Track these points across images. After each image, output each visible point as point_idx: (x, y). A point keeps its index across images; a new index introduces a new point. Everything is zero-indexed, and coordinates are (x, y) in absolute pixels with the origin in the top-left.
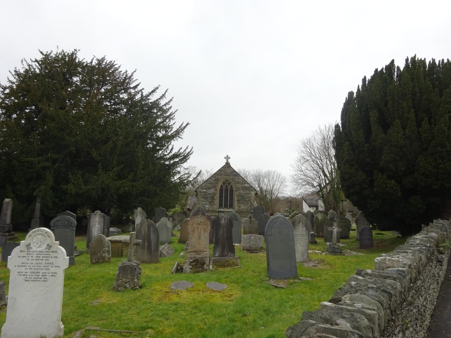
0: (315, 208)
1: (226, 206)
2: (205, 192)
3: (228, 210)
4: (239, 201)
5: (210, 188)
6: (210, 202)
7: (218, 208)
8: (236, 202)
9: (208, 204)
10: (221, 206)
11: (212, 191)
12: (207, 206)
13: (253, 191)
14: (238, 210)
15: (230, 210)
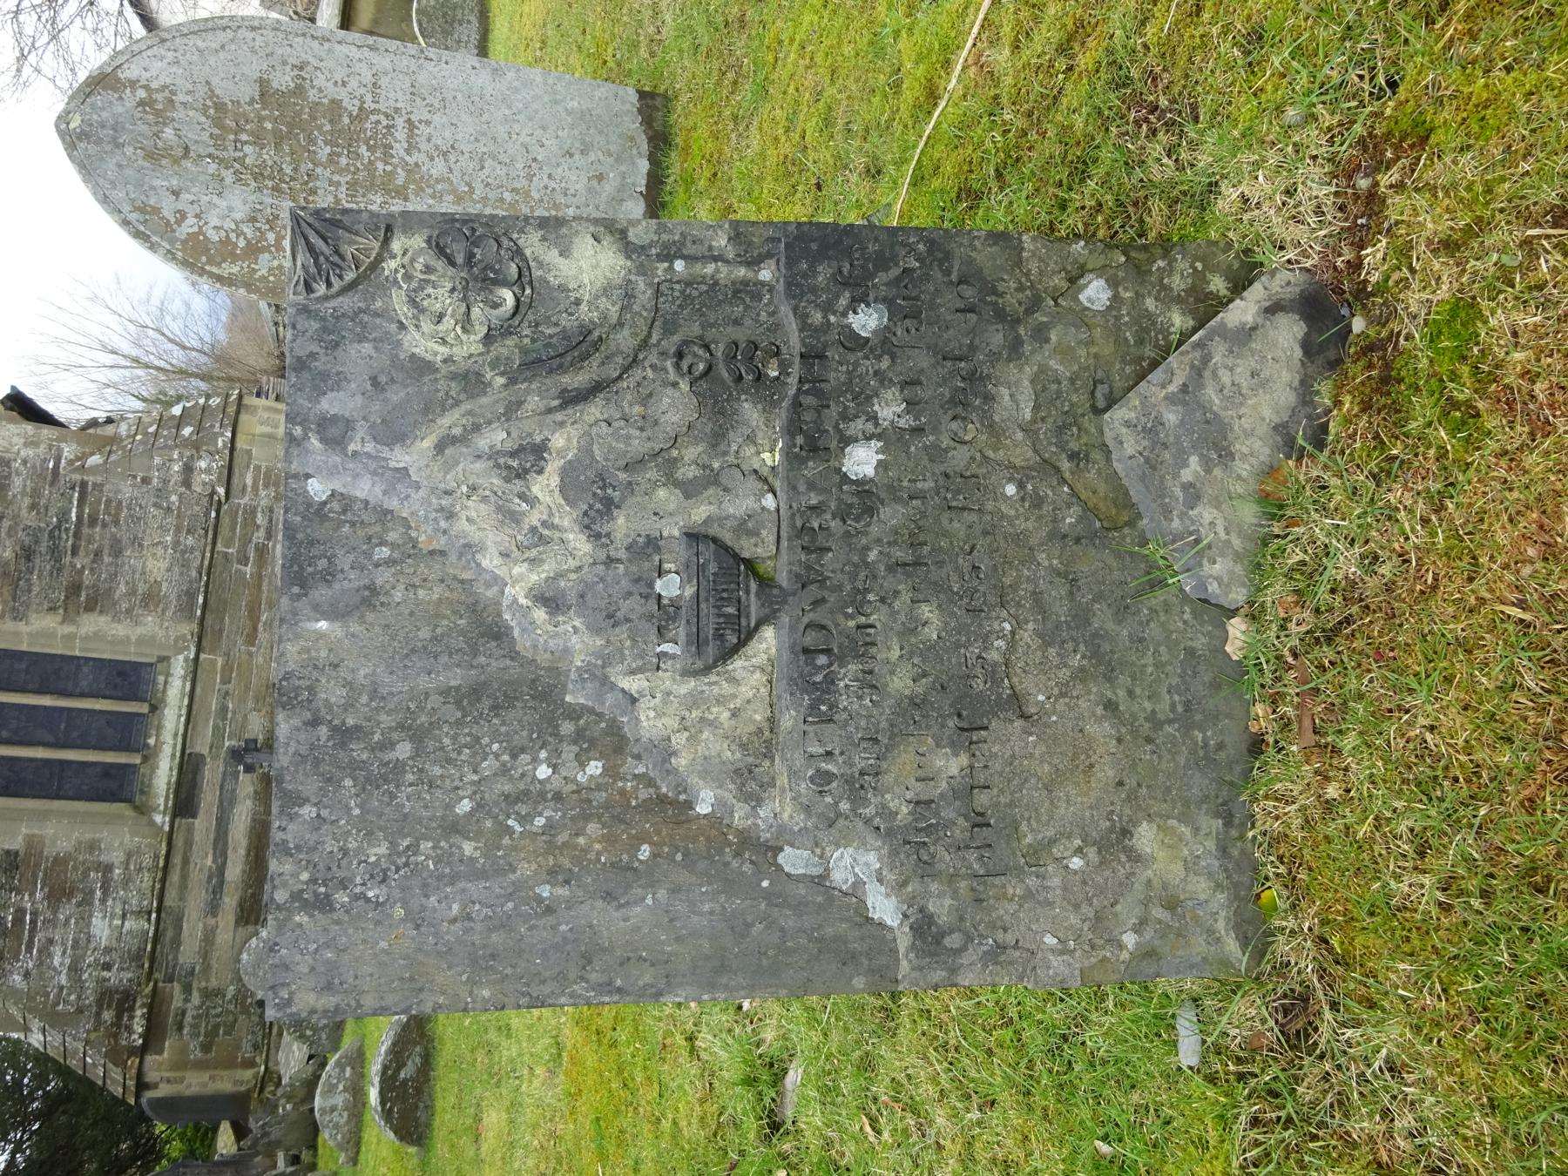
1: (130, 734)
3: (172, 718)
4: (79, 598)
6: (58, 894)
7: (143, 810)
8: (91, 624)
9: (84, 920)
10: (117, 787)
12: (101, 929)
15: (175, 689)
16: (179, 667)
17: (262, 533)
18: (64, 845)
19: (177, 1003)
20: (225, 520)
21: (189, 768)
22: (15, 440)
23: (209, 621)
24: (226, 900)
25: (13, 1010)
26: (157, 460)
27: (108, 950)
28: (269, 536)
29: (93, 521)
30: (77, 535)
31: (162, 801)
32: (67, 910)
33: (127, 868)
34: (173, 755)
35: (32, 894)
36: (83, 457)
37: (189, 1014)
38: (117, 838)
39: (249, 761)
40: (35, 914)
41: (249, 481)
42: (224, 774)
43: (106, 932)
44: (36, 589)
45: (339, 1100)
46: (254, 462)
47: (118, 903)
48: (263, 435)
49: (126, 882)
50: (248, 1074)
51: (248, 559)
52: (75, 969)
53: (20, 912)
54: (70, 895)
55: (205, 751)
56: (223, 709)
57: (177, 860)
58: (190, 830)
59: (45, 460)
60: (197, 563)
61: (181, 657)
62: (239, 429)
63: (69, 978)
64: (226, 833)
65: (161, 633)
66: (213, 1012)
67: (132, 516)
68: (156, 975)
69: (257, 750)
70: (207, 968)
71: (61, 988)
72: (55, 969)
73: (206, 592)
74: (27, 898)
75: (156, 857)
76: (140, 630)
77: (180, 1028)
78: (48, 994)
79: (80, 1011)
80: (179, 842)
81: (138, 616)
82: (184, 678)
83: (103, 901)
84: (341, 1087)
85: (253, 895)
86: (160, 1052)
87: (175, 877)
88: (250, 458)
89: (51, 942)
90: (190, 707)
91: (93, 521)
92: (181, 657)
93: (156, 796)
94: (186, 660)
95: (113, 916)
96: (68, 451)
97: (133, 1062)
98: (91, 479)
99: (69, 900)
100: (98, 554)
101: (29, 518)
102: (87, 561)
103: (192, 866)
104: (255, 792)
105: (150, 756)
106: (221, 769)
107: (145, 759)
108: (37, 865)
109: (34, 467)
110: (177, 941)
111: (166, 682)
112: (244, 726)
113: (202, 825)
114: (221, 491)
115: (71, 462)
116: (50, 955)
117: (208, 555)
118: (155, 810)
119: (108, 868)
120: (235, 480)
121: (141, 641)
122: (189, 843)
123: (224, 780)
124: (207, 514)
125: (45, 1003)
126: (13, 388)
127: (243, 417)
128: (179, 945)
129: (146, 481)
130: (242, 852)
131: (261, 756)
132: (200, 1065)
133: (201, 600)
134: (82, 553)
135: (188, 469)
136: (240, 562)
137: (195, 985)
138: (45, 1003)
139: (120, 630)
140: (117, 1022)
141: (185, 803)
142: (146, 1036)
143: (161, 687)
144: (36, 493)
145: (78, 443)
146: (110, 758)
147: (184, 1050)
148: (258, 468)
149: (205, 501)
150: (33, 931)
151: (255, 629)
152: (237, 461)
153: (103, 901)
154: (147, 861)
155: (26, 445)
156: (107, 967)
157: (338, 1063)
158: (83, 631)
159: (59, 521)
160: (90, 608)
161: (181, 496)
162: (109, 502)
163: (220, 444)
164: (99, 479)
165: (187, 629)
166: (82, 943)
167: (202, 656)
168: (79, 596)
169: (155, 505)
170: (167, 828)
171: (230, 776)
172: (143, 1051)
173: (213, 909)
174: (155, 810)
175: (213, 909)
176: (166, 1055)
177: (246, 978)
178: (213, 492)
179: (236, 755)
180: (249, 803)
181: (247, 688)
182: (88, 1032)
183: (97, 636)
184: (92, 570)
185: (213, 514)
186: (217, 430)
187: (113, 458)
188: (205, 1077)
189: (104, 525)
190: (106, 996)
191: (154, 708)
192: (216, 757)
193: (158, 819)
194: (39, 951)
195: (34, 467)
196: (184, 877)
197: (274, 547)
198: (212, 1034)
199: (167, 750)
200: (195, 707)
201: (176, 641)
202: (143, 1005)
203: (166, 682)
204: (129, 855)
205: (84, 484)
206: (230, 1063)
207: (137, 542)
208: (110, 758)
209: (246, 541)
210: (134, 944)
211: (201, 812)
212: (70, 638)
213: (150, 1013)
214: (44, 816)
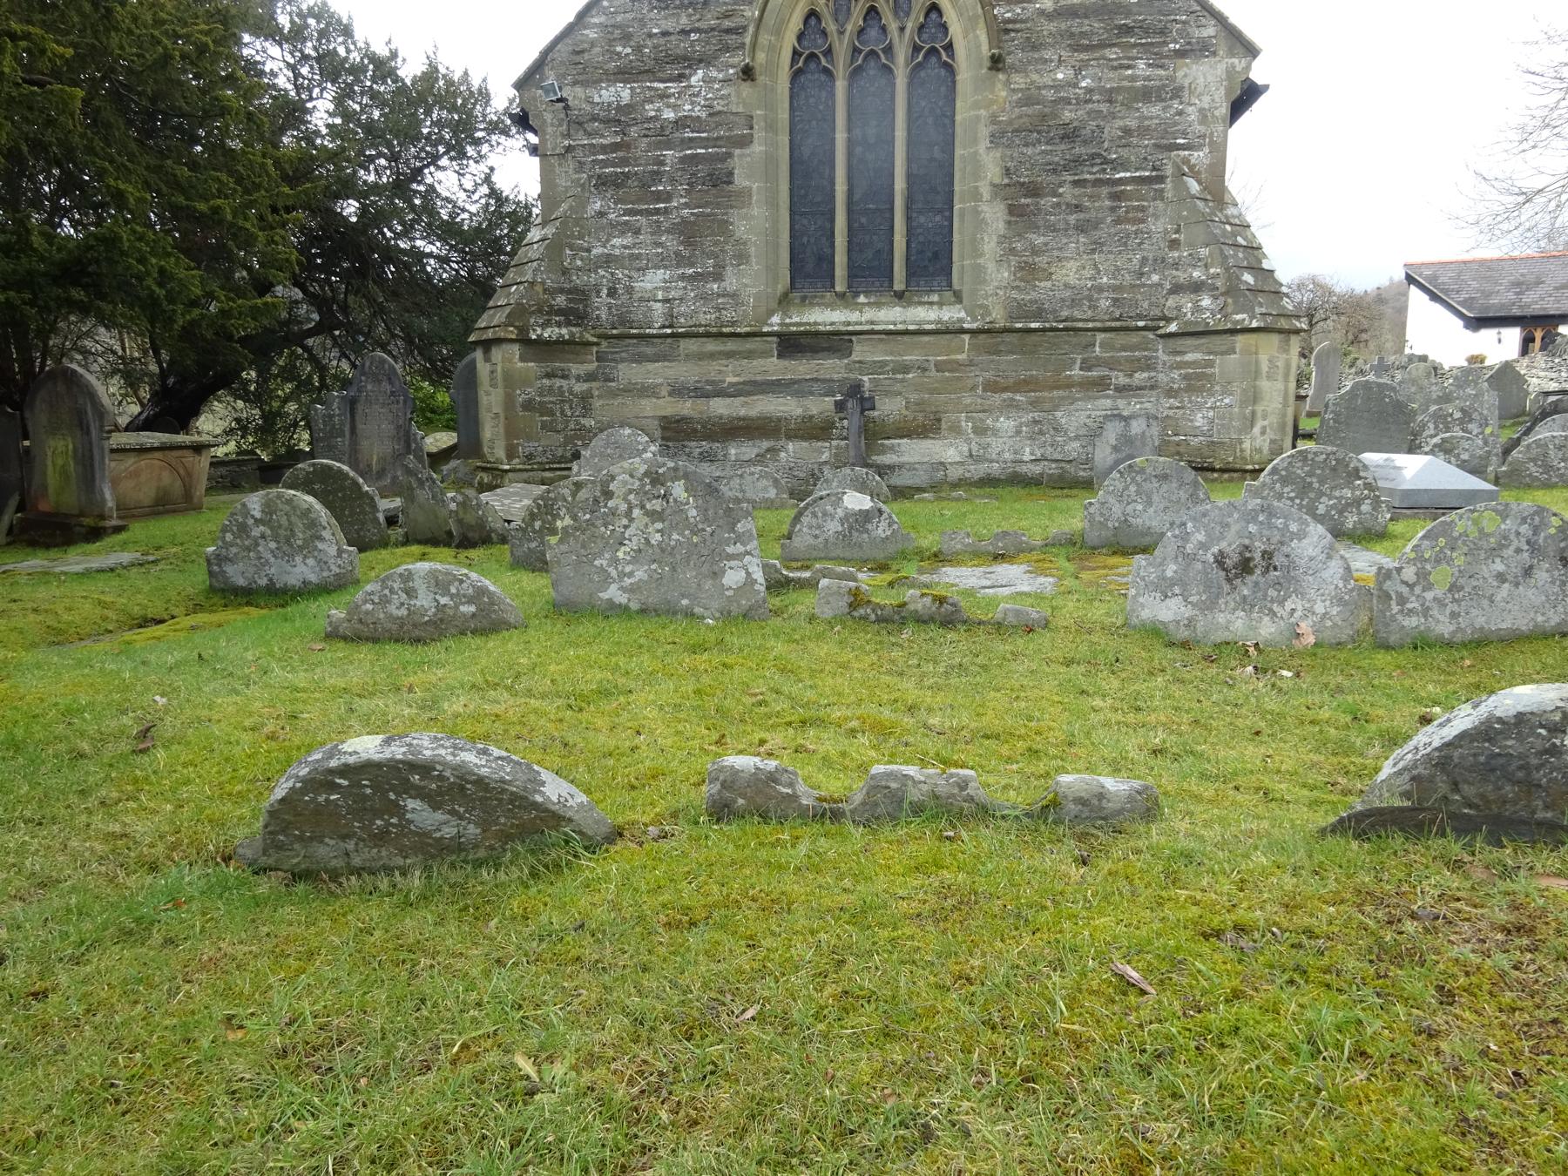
0: (1513, 335)
1: (870, 274)
2: (619, 118)
3: (891, 315)
4: (1023, 199)
5: (674, 63)
6: (688, 232)
7: (784, 302)
8: (995, 215)
10: (808, 270)
11: (701, 91)
12: (653, 281)
13: (1202, 50)
14: (1020, 311)
15: (924, 314)
16: (951, 314)
17: (1122, 380)
18: (741, 228)
19: (576, 369)
20: (1134, 338)
21: (836, 342)
22: (1206, 99)
23: (1008, 338)
24: (689, 404)
25: (564, 206)
26: (1204, 252)
27: (630, 290)
28: (1121, 390)
29: (1116, 197)
30: (1098, 183)
31: (796, 319)
32: (671, 242)
33: (719, 296)
34: (849, 324)
35: (686, 205)
36: (1196, 175)
37: (564, 383)
38: (752, 281)
39: (849, 405)
40: (666, 211)
41: (1189, 357)
42: (833, 380)
43: (649, 286)
44: (1029, 151)
45: (425, 601)
46: (1218, 360)
47: (681, 292)
48: (1257, 363)
49: (704, 297)
50: (500, 453)
51: (1089, 369)
52: (608, 260)
53: (668, 197)
54: (688, 243)
55: (855, 357)
56: (905, 369)
57: (731, 345)
58: (765, 354)
59: (1184, 134)
60: (1077, 314)
61: (963, 314)
62: (1262, 336)
63: (599, 256)
64: (763, 392)
65: (990, 289)
66: (567, 407)
67: (1128, 236)
68: (604, 343)
69: (862, 412)
70: (614, 394)
71: (588, 250)
72: (608, 241)
73: (1044, 330)
74: (683, 201)
75: (733, 324)
76: (991, 266)
77: (548, 376)
78: (581, 237)
79: (565, 272)
80: (750, 345)
81: (1009, 262)
82: (939, 322)
83: (683, 277)
84: (443, 601)
85: (695, 431)
86: (522, 359)
87: (711, 346)
88: (1223, 353)
89: (637, 232)
90: (906, 332)
91: (1116, 197)
92: (963, 314)
93: (800, 314)
94: (961, 320)
95: (666, 289)
96: (1199, 157)
97: (512, 333)
98: (1168, 185)
99: (682, 243)
100: (1078, 208)
101: (1112, 129)
102: (1069, 198)
103: (724, 362)
104: (811, 417)
105: (845, 300)
106: (835, 376)
107: (842, 296)
108: (718, 205)
109: (1176, 124)
110: (640, 359)
111: (931, 303)
112: (887, 393)
113: (773, 366)
114: (1173, 328)
115: (1186, 161)
116: (623, 233)
117: (1090, 325)
118: (785, 314)
119: (718, 277)
120: (1190, 341)
121: (979, 270)
122: (750, 355)
123: (824, 381)
124: (1140, 317)
125: (572, 236)
126: (1266, 87)
127: (1275, 339)
128: (639, 362)
129: (1174, 244)
130: (743, 412)
131: (856, 418)
132: (509, 402)
133: (1033, 325)
134: (1077, 191)
135: (1197, 287)
136: (1084, 361)
137: (594, 384)
138: (572, 236)
139: (990, 246)
140: (554, 311)
141: (792, 344)
142: (540, 342)
143: (926, 299)
144: (1143, 131)
145: (1210, 165)
146: (840, 259)
147: (526, 382)
148: (1210, 364)
149: (1157, 312)
150: (649, 213)
151: (1005, 389)
152: (1217, 339)
153: (683, 277)
154: (728, 315)
155: (1201, 110)
156: (612, 293)
157: (482, 591)
158: (984, 207)
159: (1113, 161)
160: (1012, 210)
161: (1159, 285)
162: (1143, 209)
163: (1238, 317)
164: (1169, 194)
165: (998, 316)
166: (637, 264)
167: (966, 337)
168: (1026, 196)
169: (1144, 260)
170: (765, 329)
171: (828, 387)
172: (524, 341)
173: (678, 391)
174: (785, 314)
175: (678, 391)
176: (520, 364)
177: (603, 436)
178: (1168, 320)
179: (855, 390)
180: (799, 411)
181: (932, 392)
182: (543, 283)
183: (980, 224)
184: (1058, 204)
185: (1141, 324)
186: (1258, 310)
187: (1200, 204)
188: (498, 409)
189: (1113, 209)
190: (581, 295)
191: (900, 296)
192: (848, 368)
193: (776, 319)
194: (626, 223)
195: (1176, 124)
196: (712, 356)
197: (1108, 397)
198: (544, 410)
199: (854, 316)
200: (906, 338)
201: (981, 306)
202: (572, 334)
203: (931, 303)
204: (734, 295)
205: (1161, 179)
206: (511, 432)
207: (1097, 247)
208: (840, 259)
209: (1112, 364)
210: (638, 316)
211: (786, 363)
212: (976, 195)
213: (565, 342)
214: (772, 204)
